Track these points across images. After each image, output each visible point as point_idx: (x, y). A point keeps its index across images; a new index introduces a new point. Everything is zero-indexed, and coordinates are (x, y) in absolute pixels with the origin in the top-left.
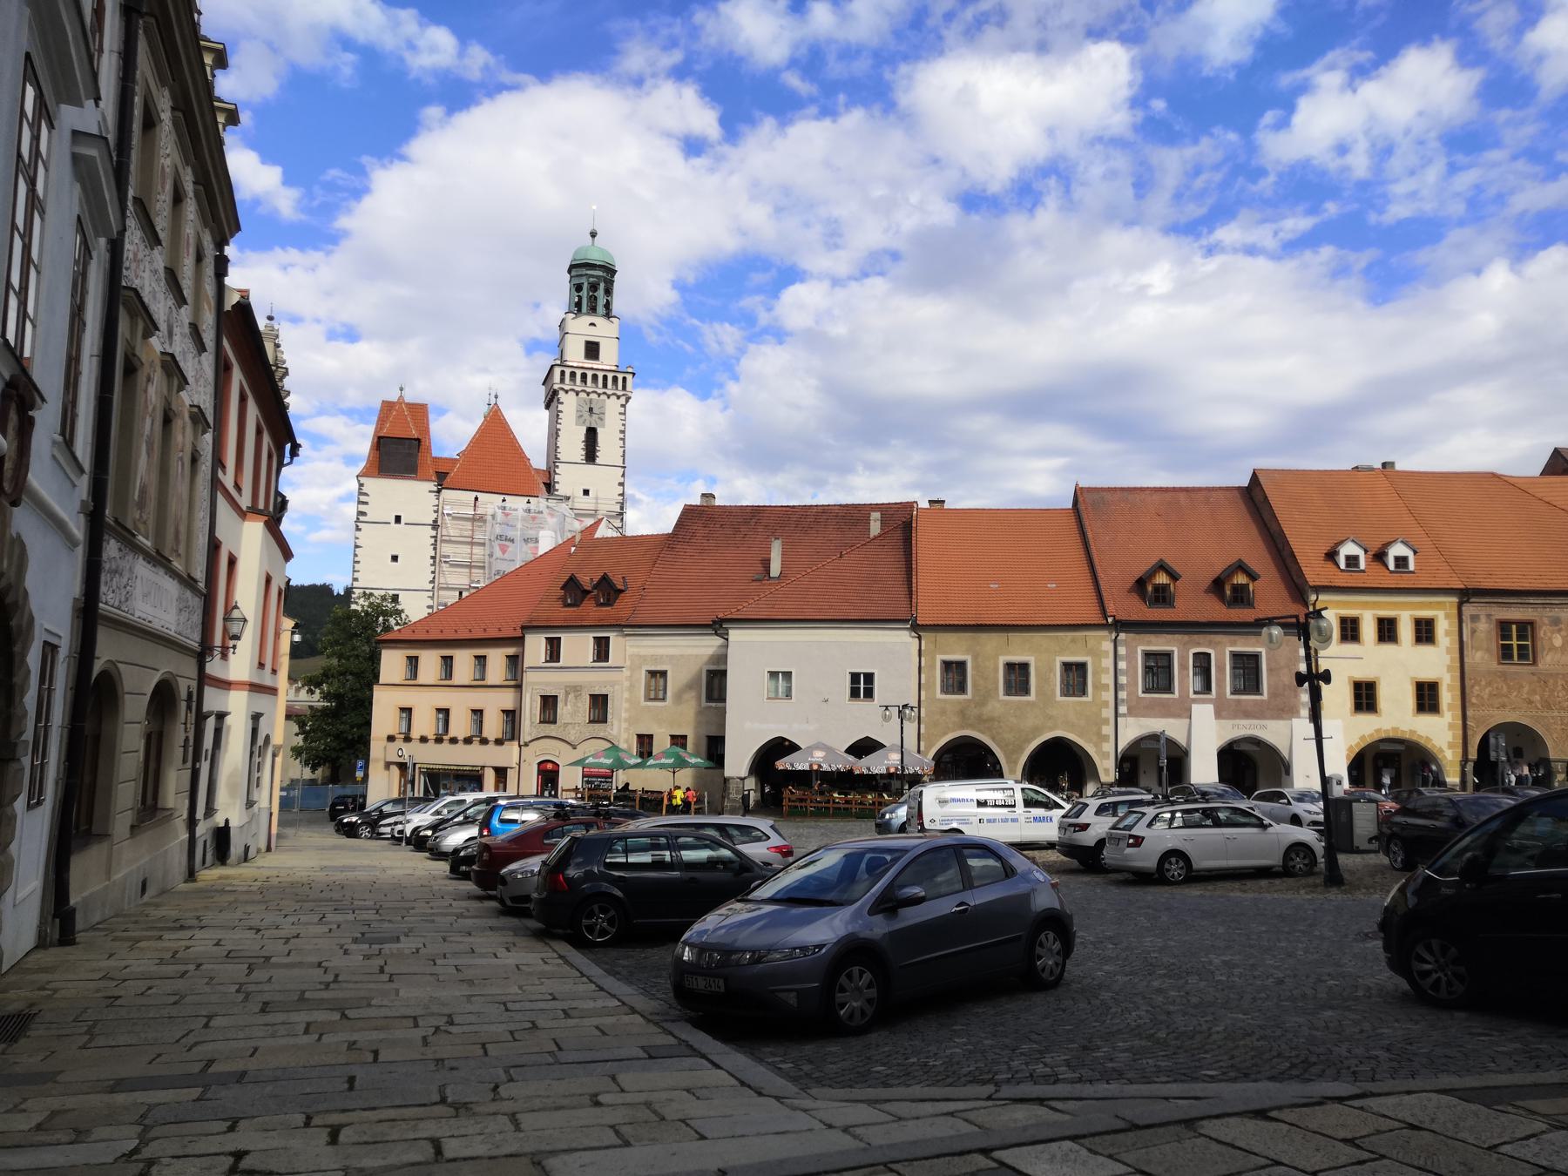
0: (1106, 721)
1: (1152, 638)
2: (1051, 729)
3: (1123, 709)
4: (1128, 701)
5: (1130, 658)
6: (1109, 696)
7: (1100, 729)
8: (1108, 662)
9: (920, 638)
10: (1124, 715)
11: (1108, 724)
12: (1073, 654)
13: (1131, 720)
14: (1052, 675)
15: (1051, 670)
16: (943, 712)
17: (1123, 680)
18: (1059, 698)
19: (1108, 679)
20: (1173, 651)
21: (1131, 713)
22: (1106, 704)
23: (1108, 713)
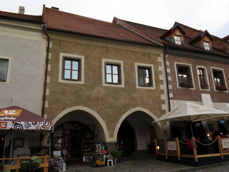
0: (163, 102)
1: (181, 59)
2: (135, 106)
3: (171, 95)
4: (173, 91)
5: (172, 67)
6: (163, 87)
7: (161, 107)
8: (161, 68)
9: (48, 40)
10: (172, 98)
11: (164, 104)
12: (143, 62)
13: (175, 101)
14: (133, 73)
15: (133, 70)
16: (63, 93)
17: (170, 78)
18: (138, 87)
19: (162, 77)
20: (190, 66)
21: (174, 98)
22: (162, 92)
23: (164, 97)
